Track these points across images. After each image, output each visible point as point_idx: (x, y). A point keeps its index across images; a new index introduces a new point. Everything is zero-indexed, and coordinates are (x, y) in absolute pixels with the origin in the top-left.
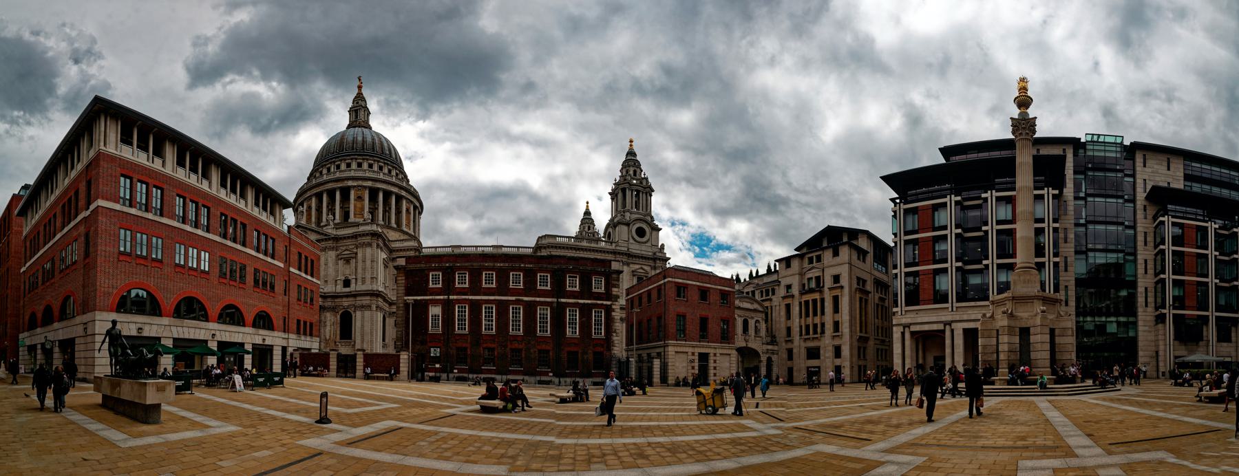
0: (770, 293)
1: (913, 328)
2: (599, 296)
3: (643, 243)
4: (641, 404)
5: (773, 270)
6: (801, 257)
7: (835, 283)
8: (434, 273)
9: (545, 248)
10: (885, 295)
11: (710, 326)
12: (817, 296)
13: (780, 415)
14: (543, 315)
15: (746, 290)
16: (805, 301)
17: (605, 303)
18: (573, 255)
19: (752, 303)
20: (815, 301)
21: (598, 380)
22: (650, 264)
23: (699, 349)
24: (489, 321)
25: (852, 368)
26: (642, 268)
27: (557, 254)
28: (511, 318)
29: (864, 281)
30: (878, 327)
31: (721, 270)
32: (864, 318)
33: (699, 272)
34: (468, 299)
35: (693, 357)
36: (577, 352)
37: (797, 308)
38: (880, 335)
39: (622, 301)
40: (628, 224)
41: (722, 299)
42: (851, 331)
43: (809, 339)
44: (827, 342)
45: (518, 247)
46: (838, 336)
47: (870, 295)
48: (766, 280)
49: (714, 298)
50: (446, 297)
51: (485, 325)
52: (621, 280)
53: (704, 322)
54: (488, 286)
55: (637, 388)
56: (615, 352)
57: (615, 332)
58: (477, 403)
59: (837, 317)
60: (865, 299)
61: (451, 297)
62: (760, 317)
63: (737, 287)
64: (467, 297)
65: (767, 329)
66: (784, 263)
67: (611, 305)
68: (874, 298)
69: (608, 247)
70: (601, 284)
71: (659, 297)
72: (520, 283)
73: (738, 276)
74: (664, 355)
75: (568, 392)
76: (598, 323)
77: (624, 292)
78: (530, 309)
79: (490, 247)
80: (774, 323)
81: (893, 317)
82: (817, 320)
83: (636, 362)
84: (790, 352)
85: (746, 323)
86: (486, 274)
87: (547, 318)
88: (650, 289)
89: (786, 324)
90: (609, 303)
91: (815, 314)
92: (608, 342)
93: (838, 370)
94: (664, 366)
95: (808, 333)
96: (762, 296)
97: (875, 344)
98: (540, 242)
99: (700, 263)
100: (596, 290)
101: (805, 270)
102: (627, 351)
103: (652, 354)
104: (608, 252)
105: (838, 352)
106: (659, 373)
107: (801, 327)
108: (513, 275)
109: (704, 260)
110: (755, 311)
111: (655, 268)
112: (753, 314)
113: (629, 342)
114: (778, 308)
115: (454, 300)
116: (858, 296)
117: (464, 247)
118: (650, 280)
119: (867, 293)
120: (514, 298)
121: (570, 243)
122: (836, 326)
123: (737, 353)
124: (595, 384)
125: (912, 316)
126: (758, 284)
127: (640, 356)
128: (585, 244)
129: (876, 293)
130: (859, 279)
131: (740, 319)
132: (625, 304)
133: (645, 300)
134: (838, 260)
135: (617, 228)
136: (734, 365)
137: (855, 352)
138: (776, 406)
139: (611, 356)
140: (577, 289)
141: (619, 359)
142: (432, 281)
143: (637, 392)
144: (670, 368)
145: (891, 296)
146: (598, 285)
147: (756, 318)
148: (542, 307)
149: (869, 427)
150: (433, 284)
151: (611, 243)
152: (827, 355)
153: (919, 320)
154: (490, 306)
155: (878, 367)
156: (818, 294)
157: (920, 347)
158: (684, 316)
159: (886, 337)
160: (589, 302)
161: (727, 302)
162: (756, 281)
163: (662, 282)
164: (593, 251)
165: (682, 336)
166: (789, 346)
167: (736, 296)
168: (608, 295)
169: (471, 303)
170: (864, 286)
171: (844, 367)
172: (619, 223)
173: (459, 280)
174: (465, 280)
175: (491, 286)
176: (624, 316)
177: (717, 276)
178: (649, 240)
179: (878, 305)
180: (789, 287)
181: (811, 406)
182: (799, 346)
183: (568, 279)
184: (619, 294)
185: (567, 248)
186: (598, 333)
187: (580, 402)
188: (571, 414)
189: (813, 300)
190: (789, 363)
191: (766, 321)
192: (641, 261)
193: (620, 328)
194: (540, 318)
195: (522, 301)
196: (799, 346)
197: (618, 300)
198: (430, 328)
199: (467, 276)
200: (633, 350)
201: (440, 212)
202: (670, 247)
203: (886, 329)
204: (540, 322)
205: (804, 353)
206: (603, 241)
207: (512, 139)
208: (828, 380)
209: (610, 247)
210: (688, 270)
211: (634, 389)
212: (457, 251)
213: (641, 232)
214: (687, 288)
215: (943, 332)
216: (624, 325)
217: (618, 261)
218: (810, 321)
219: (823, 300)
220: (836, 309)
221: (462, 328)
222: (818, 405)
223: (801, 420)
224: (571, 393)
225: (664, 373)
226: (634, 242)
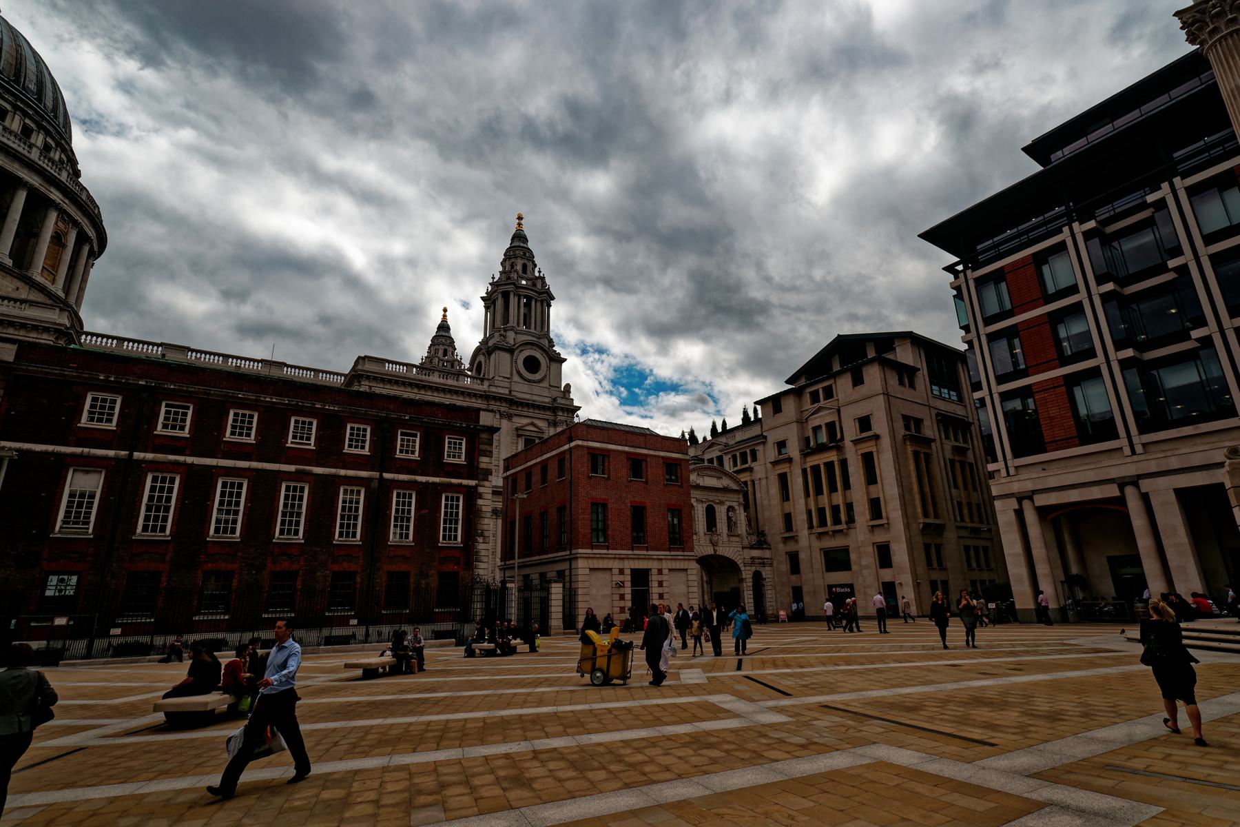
0: (749, 459)
1: (1041, 500)
2: (454, 471)
3: (534, 382)
4: (524, 671)
5: (752, 419)
6: (797, 393)
7: (862, 431)
8: (101, 395)
9: (368, 378)
10: (965, 441)
11: (649, 520)
12: (832, 456)
13: (785, 684)
14: (351, 502)
15: (707, 456)
16: (811, 467)
17: (465, 482)
18: (412, 396)
19: (719, 478)
20: (829, 466)
21: (447, 626)
22: (546, 417)
23: (631, 562)
24: (228, 512)
25: (917, 585)
26: (533, 424)
27: (385, 392)
28: (281, 508)
29: (919, 422)
30: (960, 504)
31: (665, 425)
32: (927, 489)
33: (627, 429)
34: (185, 464)
35: (621, 578)
36: (407, 574)
37: (800, 480)
38: (967, 518)
39: (497, 480)
40: (511, 351)
41: (667, 474)
42: (905, 515)
43: (826, 533)
44: (861, 538)
45: (317, 371)
46: (882, 525)
47: (933, 444)
48: (739, 436)
49: (654, 472)
50: (123, 453)
51: (218, 521)
52: (495, 444)
53: (639, 513)
54: (236, 439)
55: (518, 641)
56: (481, 572)
57: (482, 535)
58: (157, 708)
59: (875, 491)
60: (925, 453)
61: (137, 455)
62: (735, 500)
63: (692, 452)
64: (181, 458)
65: (749, 521)
66: (770, 405)
67: (477, 486)
68: (943, 449)
69: (476, 387)
70: (460, 449)
71: (561, 473)
72: (309, 439)
73: (692, 433)
74: (571, 575)
75: (382, 655)
76: (451, 519)
77: (502, 463)
78: (325, 491)
79: (258, 361)
80: (759, 508)
81: (991, 482)
82: (838, 499)
83: (519, 590)
84: (794, 559)
85: (710, 513)
86: (236, 415)
87: (357, 509)
88: (547, 459)
89: (782, 509)
90: (472, 483)
91: (833, 488)
92: (468, 553)
93: (889, 590)
94: (570, 595)
95: (823, 522)
96: (735, 465)
97: (959, 537)
98: (359, 367)
99: (630, 414)
100: (451, 460)
101: (806, 414)
102: (503, 569)
103: (549, 575)
104: (475, 395)
105: (884, 556)
106: (560, 609)
107: (809, 512)
108: (296, 422)
109: (635, 409)
110: (725, 490)
111: (554, 424)
112: (721, 497)
113: (507, 554)
114: (764, 482)
115: (144, 461)
116: (910, 449)
117: (197, 351)
118: (547, 444)
119: (928, 442)
120: (292, 468)
121: (409, 375)
122: (876, 507)
123: (699, 566)
124: (438, 635)
125: (1034, 476)
126: (726, 445)
127: (526, 578)
128: (435, 378)
129: (944, 441)
130: (906, 418)
131: (700, 506)
132: (502, 485)
133: (536, 478)
134: (863, 390)
135: (493, 356)
136: (695, 589)
137: (920, 555)
138: (775, 664)
139: (474, 580)
140: (416, 456)
141: (488, 585)
142: (90, 412)
143: (519, 649)
144: (580, 598)
145: (978, 443)
146: (455, 452)
147: (728, 504)
148: (349, 488)
149: (983, 714)
150: (92, 419)
151: (482, 380)
152: (864, 562)
153: (1053, 482)
154: (237, 481)
155: (973, 583)
156: (834, 453)
157: (1067, 538)
158: (605, 506)
159: (981, 522)
160: (437, 480)
161: (677, 477)
162: (723, 440)
163: (566, 447)
164: (450, 391)
165: (601, 539)
166: (791, 547)
167: (691, 467)
168: (472, 469)
169: (190, 473)
170: (918, 429)
171: (901, 584)
172: (496, 348)
173: (166, 419)
174: (184, 421)
175: (244, 439)
176: (499, 505)
177: (659, 436)
178: (545, 376)
179: (952, 462)
180: (781, 445)
181: (848, 661)
182: (809, 545)
183: (399, 437)
184: (490, 467)
185: (404, 384)
186: (451, 536)
187: (406, 673)
188: (383, 703)
189: (826, 464)
190: (794, 577)
191: (746, 507)
192: (531, 412)
193: (492, 527)
194: (344, 509)
195: (310, 474)
196: (809, 545)
197: (490, 477)
198: (59, 524)
199: (190, 413)
200: (514, 568)
201: (143, 264)
202: (579, 389)
203: (978, 505)
204: (342, 518)
205: (819, 561)
206: (468, 376)
207: (320, 179)
208: (872, 611)
209: (480, 387)
210: (610, 426)
211: (513, 642)
212: (173, 357)
213: (532, 365)
214: (608, 456)
215: (1121, 501)
216: (500, 521)
217: (492, 411)
218: (824, 500)
219: (844, 464)
220: (871, 477)
221: (154, 523)
222: (864, 660)
223: (833, 691)
224: (388, 657)
225: (570, 608)
226: (520, 381)
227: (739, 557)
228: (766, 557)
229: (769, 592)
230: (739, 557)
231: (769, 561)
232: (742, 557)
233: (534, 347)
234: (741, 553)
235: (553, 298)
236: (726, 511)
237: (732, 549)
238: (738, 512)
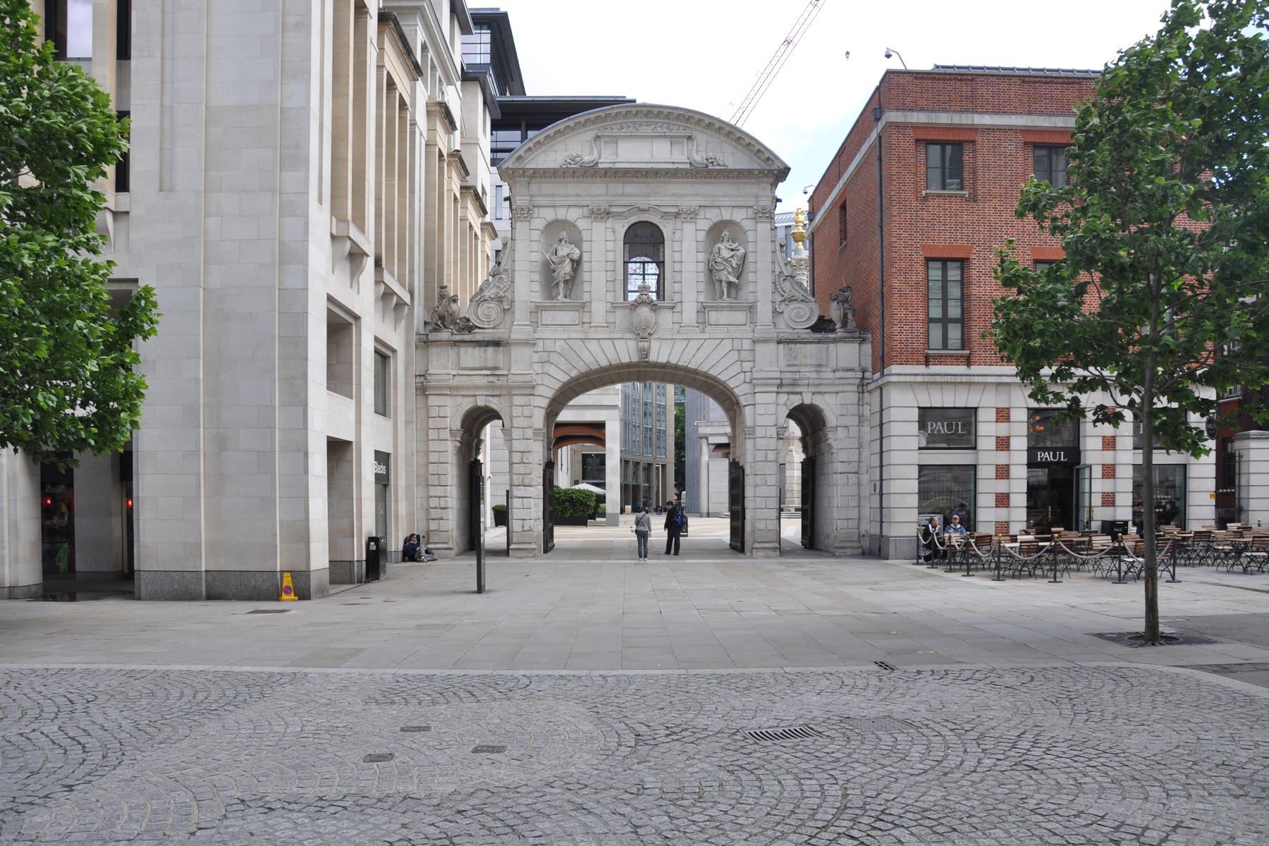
236: (702, 236)
237: (710, 345)
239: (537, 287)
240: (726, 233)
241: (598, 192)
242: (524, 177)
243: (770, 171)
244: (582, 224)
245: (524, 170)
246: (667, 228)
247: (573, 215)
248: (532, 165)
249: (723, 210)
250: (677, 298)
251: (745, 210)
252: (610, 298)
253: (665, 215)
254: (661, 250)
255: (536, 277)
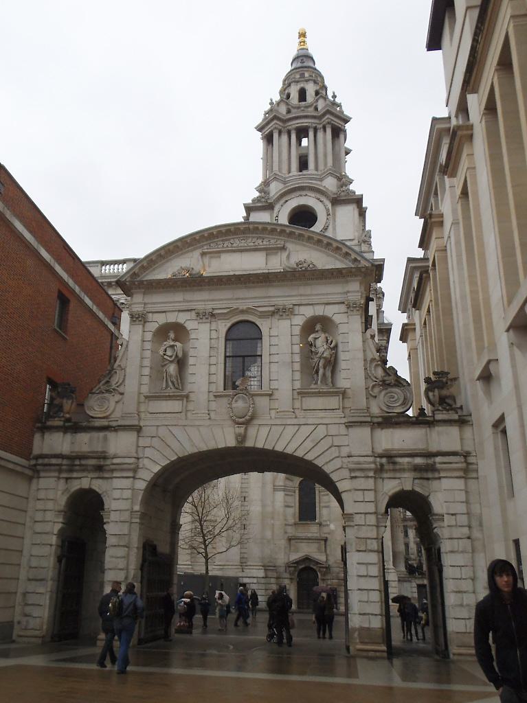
227: (334, 452)
228: (445, 448)
229: (459, 559)
230: (334, 452)
231: (458, 462)
232: (345, 451)
233: (304, 193)
234: (344, 440)
235: (346, 120)
236: (297, 330)
237: (305, 430)
238: (342, 329)
239: (146, 380)
240: (318, 327)
241: (203, 300)
242: (139, 288)
243: (358, 269)
244: (189, 325)
245: (141, 282)
246: (264, 325)
247: (182, 318)
248: (145, 279)
249: (317, 307)
250: (274, 385)
251: (337, 306)
252: (213, 388)
253: (264, 315)
254: (259, 345)
255: (146, 371)
